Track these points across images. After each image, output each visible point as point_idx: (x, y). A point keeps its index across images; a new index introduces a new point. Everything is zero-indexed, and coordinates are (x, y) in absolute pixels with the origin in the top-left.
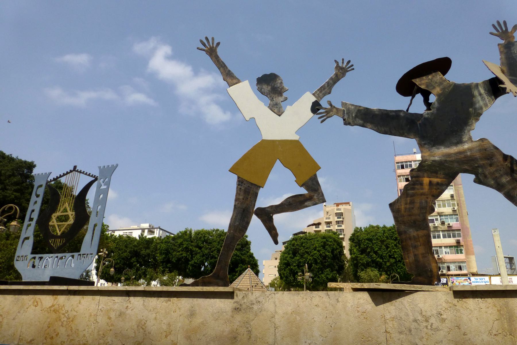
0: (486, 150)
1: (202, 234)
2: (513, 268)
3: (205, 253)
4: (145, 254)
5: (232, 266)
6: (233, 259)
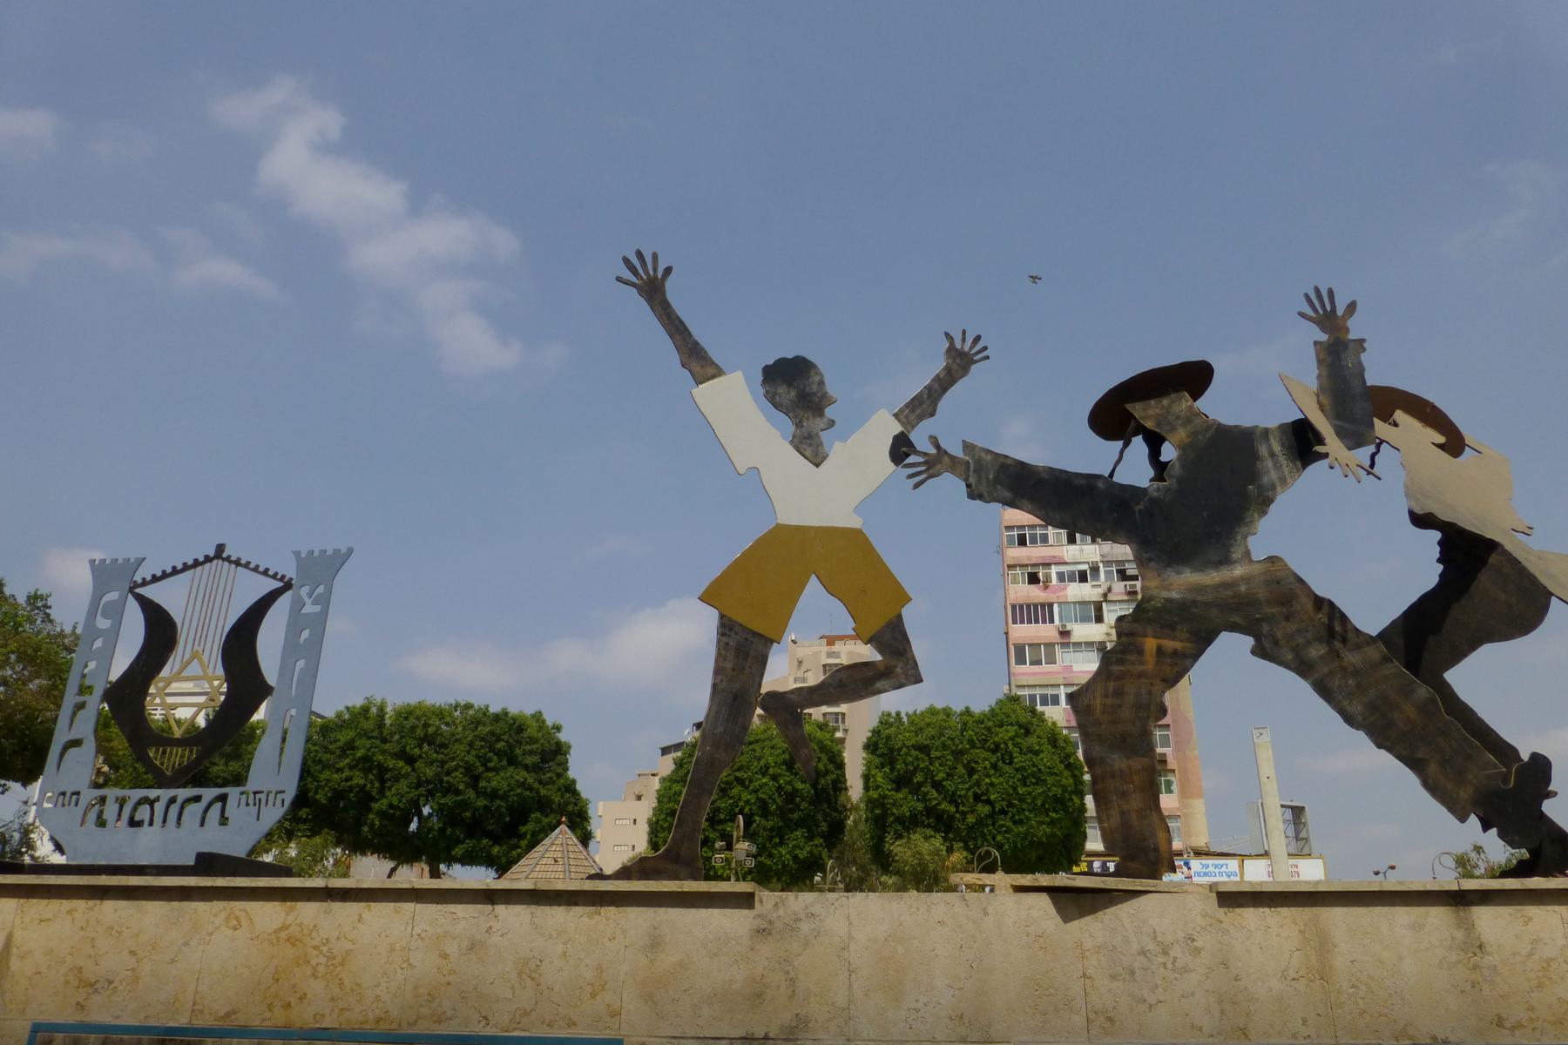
0: (1278, 583)
1: (418, 718)
3: (425, 776)
4: (225, 775)
5: (508, 819)
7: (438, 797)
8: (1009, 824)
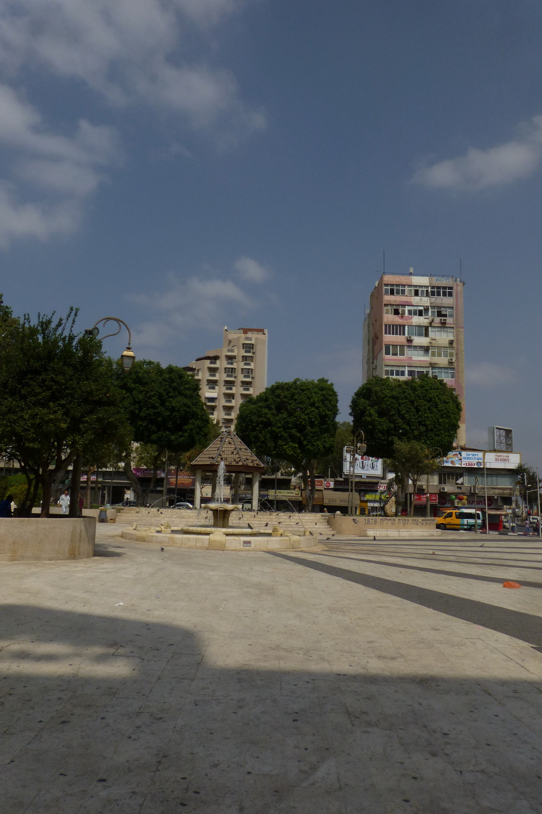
2: (508, 443)
8: (433, 436)
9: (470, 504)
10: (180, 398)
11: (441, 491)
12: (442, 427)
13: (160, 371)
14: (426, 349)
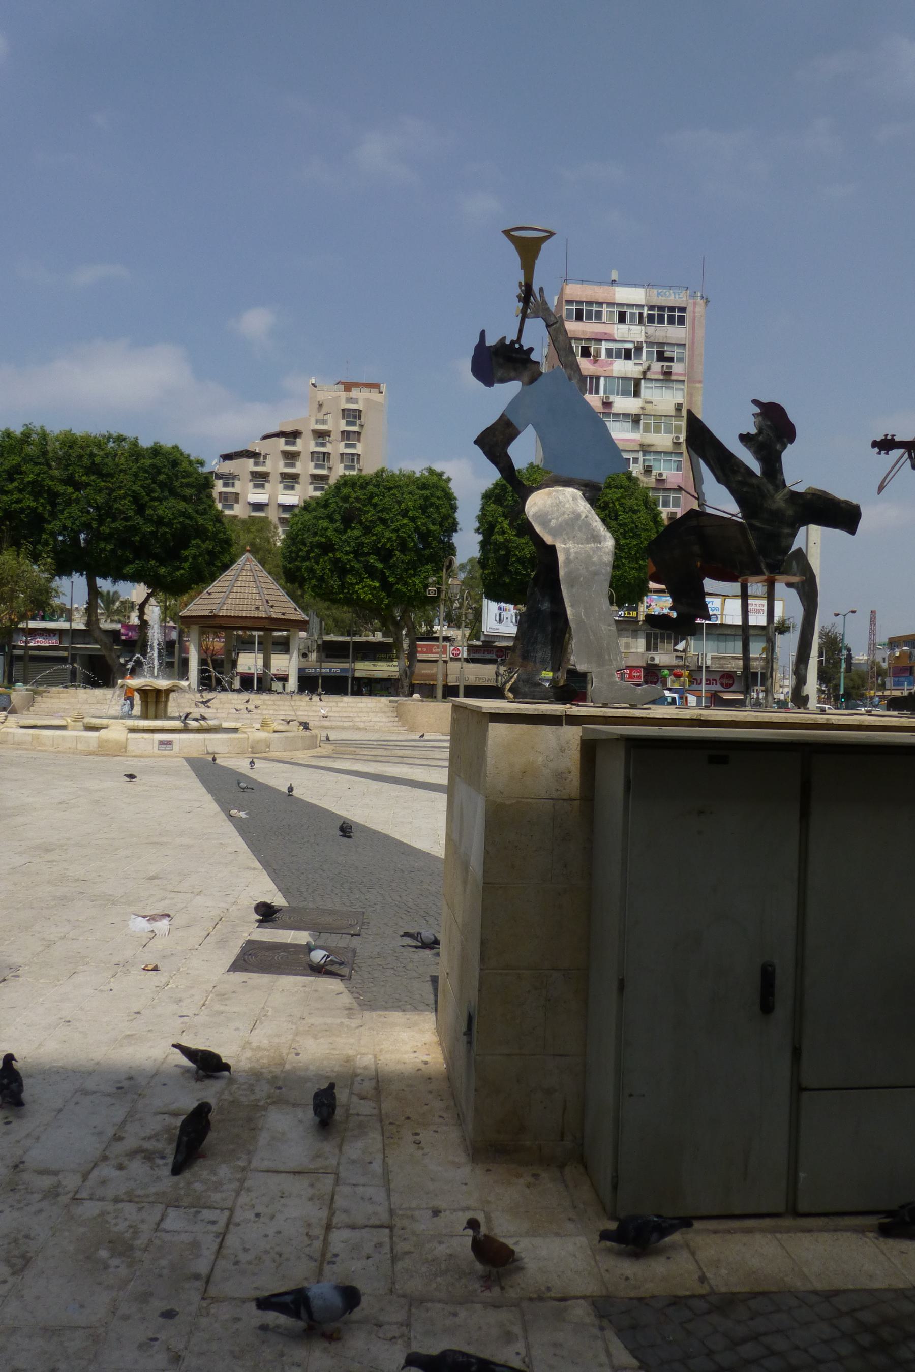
5: (172, 544)
6: (177, 523)
7: (109, 522)
9: (697, 684)
10: (173, 501)
11: (649, 662)
12: (625, 553)
13: (136, 453)
14: (636, 420)
